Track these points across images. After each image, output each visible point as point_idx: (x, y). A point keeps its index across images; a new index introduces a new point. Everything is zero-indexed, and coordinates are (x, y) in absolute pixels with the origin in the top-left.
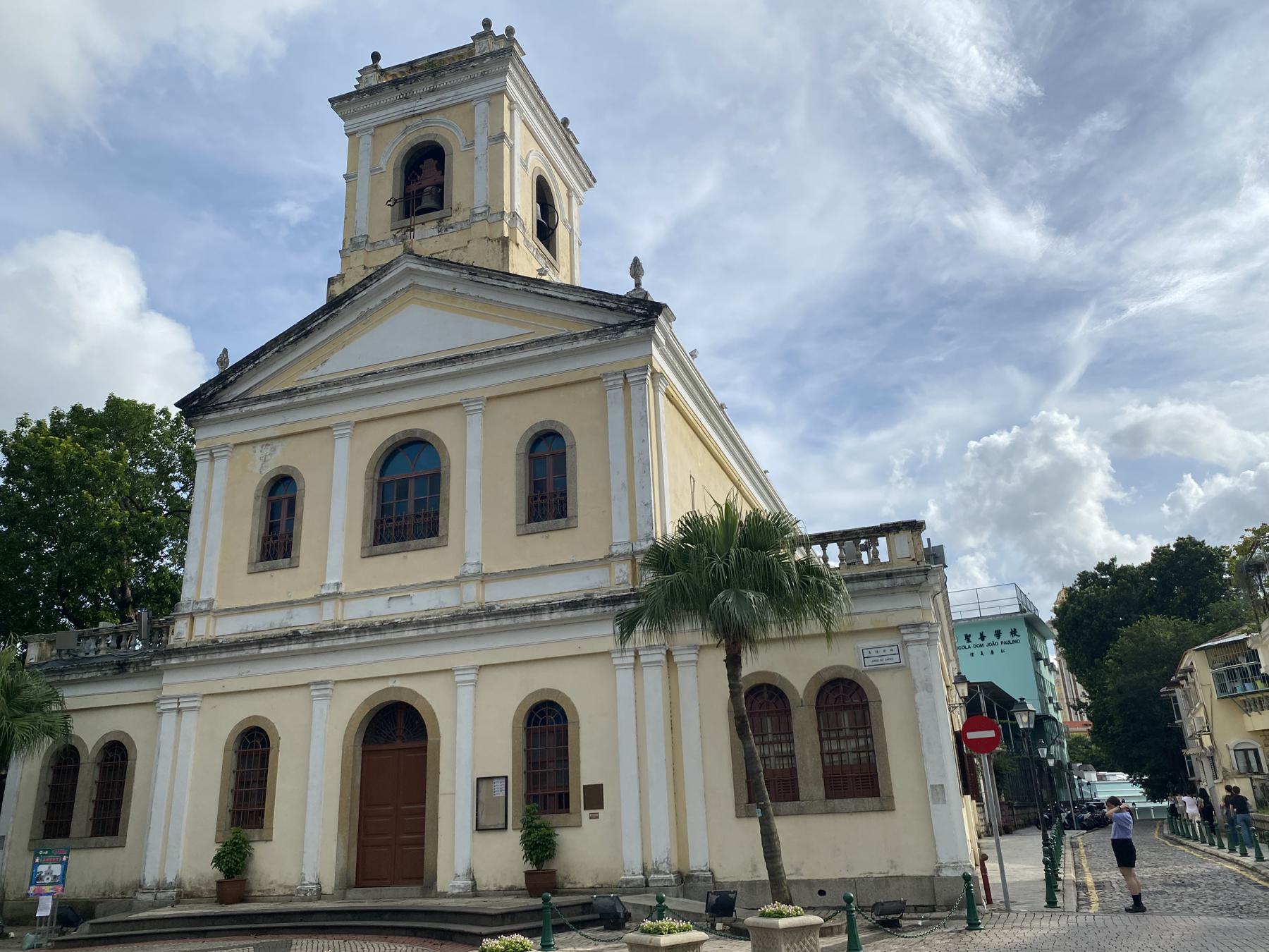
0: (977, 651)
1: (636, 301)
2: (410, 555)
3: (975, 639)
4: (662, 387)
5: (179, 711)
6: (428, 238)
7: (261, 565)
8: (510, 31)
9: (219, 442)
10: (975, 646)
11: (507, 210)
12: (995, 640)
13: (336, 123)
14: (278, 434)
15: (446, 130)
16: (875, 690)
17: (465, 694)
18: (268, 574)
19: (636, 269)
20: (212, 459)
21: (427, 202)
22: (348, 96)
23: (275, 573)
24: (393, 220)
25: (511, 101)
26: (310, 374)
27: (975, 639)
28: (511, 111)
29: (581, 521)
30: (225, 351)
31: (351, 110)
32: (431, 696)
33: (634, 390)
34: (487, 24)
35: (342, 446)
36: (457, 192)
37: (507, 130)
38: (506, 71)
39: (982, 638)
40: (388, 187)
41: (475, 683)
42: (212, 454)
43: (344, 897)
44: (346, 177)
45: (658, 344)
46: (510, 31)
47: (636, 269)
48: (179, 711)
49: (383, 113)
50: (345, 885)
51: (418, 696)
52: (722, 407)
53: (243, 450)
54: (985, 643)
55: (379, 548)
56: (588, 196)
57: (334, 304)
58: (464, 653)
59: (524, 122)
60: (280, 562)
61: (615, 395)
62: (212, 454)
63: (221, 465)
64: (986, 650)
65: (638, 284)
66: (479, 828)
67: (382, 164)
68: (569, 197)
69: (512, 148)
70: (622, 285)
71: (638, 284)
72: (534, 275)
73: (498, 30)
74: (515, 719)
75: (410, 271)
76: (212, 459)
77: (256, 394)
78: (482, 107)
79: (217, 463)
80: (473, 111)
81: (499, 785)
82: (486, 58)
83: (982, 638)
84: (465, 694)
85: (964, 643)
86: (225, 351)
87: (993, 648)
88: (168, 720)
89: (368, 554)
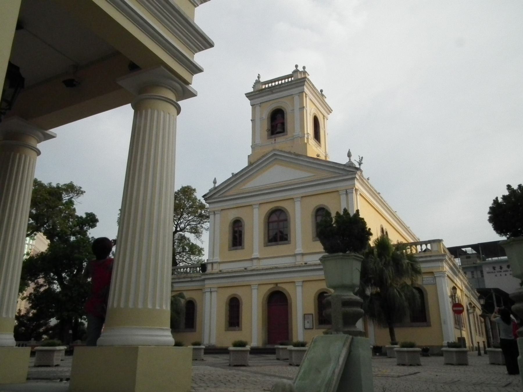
0: (498, 274)
1: (350, 167)
2: (279, 246)
3: (498, 269)
4: (358, 193)
5: (211, 292)
6: (281, 143)
7: (233, 248)
8: (304, 68)
9: (217, 209)
10: (498, 272)
11: (306, 132)
12: (507, 269)
13: (248, 102)
15: (286, 105)
16: (426, 291)
17: (299, 290)
18: (234, 251)
19: (349, 155)
20: (215, 214)
21: (278, 130)
22: (252, 92)
24: (268, 136)
25: (306, 94)
26: (244, 187)
27: (498, 269)
28: (306, 97)
30: (215, 179)
31: (252, 98)
32: (287, 288)
33: (349, 195)
34: (296, 66)
35: (256, 211)
36: (289, 126)
37: (305, 105)
38: (304, 85)
39: (501, 268)
40: (266, 125)
41: (302, 286)
44: (252, 120)
45: (357, 179)
46: (304, 68)
47: (349, 155)
48: (211, 292)
49: (262, 98)
50: (265, 344)
51: (284, 289)
52: (379, 193)
53: (224, 211)
54: (502, 270)
55: (270, 244)
56: (330, 116)
57: (250, 164)
58: (298, 277)
59: (310, 100)
60: (238, 247)
61: (343, 197)
63: (218, 216)
64: (503, 274)
65: (350, 159)
67: (264, 117)
68: (324, 119)
69: (307, 110)
70: (343, 160)
71: (350, 159)
72: (315, 157)
73: (300, 69)
74: (315, 297)
75: (275, 155)
76: (215, 214)
78: (296, 98)
79: (216, 215)
80: (293, 98)
81: (311, 316)
82: (297, 81)
83: (501, 268)
84: (299, 290)
85: (492, 270)
86: (215, 179)
87: (506, 273)
88: (208, 295)
89: (266, 245)
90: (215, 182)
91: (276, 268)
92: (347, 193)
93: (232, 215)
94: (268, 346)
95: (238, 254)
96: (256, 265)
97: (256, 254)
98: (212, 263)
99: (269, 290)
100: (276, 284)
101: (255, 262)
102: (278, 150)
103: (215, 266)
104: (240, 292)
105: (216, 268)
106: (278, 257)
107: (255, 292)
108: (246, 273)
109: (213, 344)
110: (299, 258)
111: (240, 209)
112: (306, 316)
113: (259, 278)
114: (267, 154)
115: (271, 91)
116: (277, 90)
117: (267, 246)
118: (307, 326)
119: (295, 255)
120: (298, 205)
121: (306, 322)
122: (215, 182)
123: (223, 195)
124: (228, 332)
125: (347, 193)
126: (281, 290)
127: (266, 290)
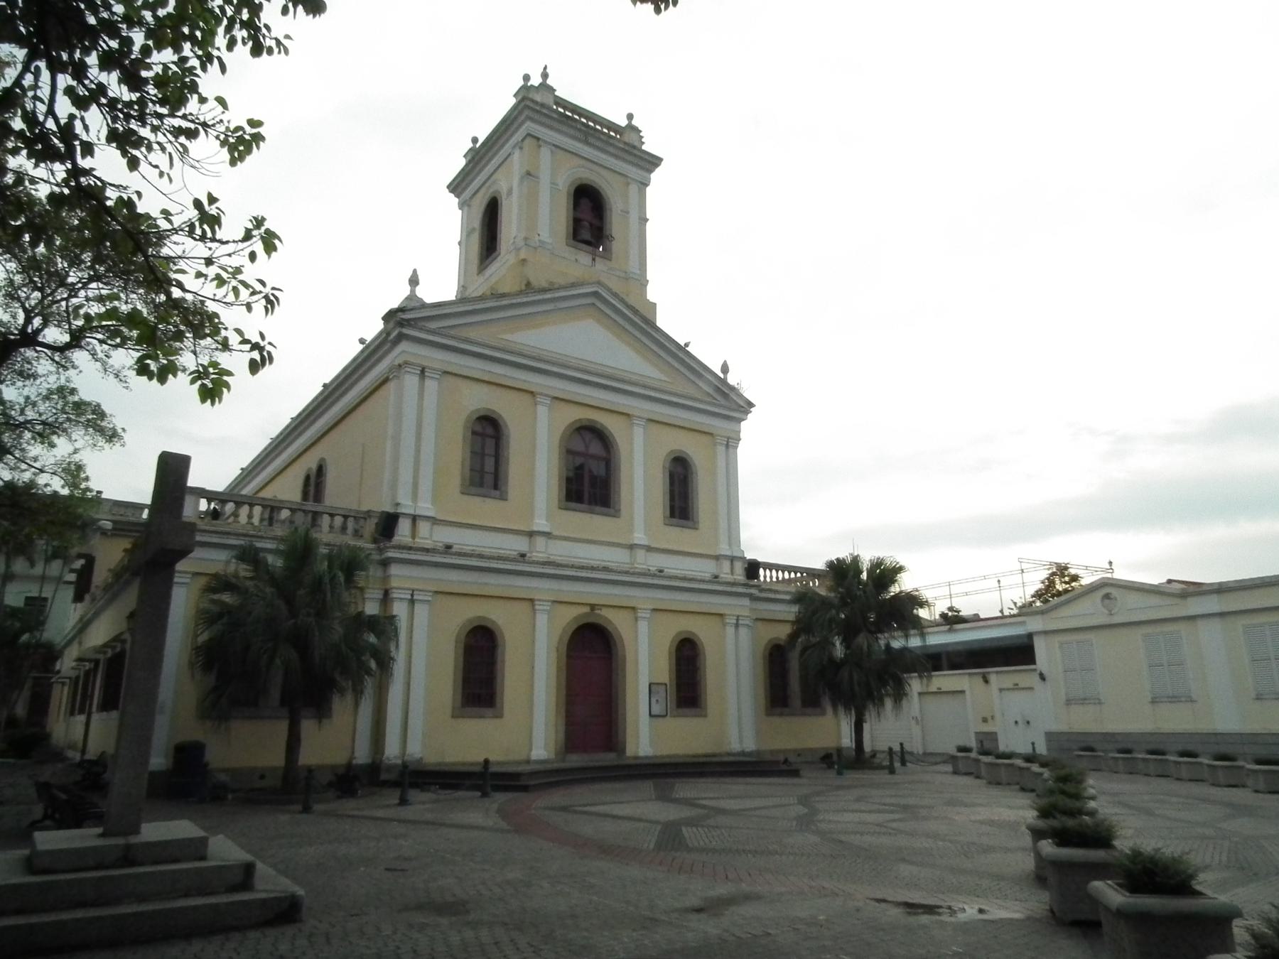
5: (412, 602)
14: (486, 378)
17: (643, 627)
23: (488, 500)
26: (508, 337)
29: (701, 525)
30: (415, 271)
32: (618, 622)
33: (731, 450)
42: (423, 371)
43: (563, 760)
58: (644, 599)
61: (721, 449)
62: (423, 371)
66: (650, 715)
77: (452, 332)
78: (633, 188)
79: (428, 382)
86: (415, 271)
90: (414, 281)
91: (606, 569)
92: (727, 446)
93: (476, 399)
94: (575, 760)
95: (484, 509)
96: (541, 550)
97: (541, 524)
98: (415, 519)
99: (576, 618)
100: (593, 607)
101: (540, 542)
102: (609, 290)
103: (423, 528)
104: (496, 614)
105: (428, 536)
106: (583, 540)
107: (542, 620)
108: (519, 565)
109: (418, 756)
110: (640, 554)
111: (499, 391)
112: (653, 688)
113: (554, 585)
114: (582, 284)
115: (586, 134)
116: (598, 144)
117: (566, 509)
118: (657, 709)
119: (632, 547)
120: (638, 433)
121: (653, 700)
122: (414, 281)
123: (452, 332)
124: (460, 720)
125: (727, 446)
126: (601, 622)
127: (568, 617)
